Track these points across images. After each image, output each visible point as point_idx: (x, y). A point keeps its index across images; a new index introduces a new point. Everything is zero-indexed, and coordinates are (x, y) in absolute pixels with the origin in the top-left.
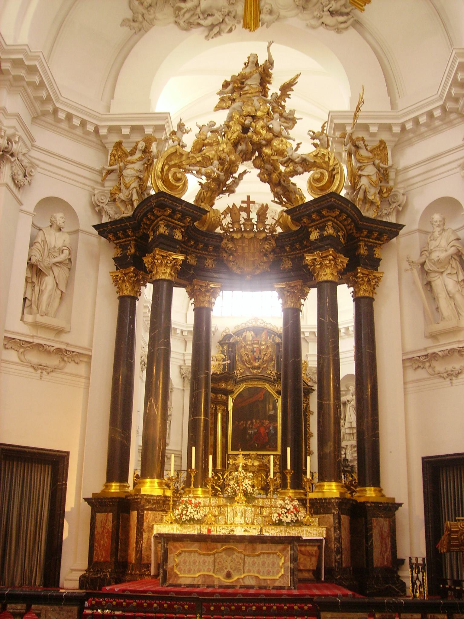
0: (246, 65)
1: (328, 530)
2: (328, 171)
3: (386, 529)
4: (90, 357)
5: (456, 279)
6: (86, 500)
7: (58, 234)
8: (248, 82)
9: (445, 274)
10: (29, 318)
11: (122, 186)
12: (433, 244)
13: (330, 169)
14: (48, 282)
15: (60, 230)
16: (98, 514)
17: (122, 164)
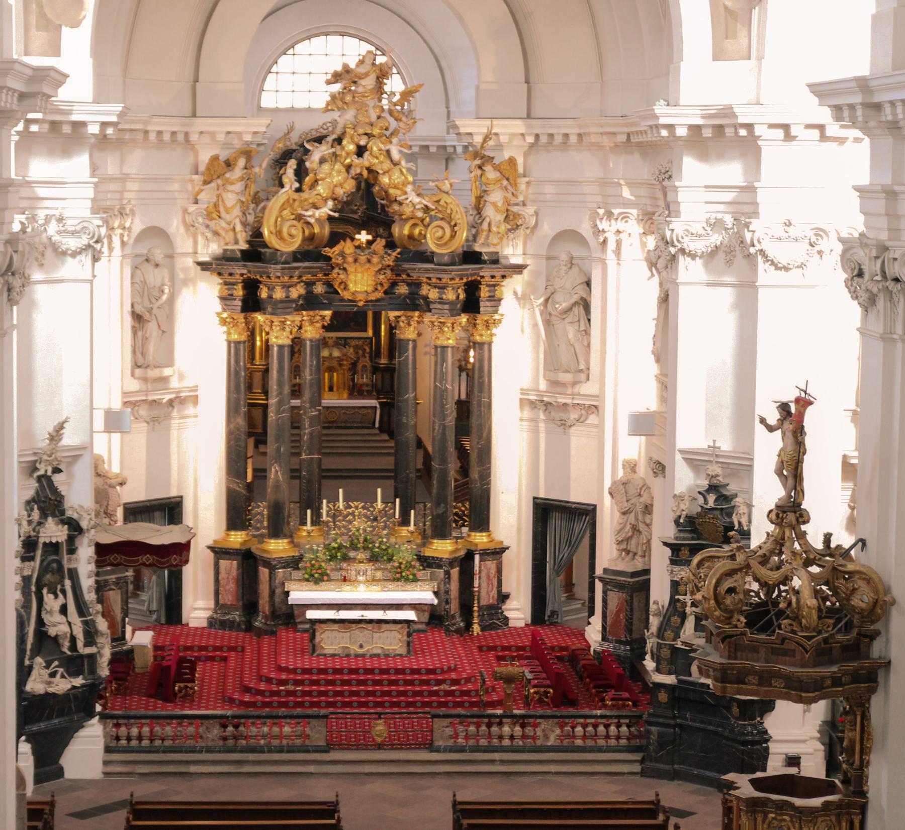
0: (361, 62)
1: (439, 585)
2: (449, 223)
3: (493, 570)
4: (197, 396)
5: (577, 328)
6: (209, 547)
7: (156, 270)
8: (363, 82)
9: (567, 320)
10: (138, 372)
11: (222, 209)
12: (558, 283)
13: (453, 223)
14: (152, 326)
15: (157, 265)
16: (221, 561)
17: (220, 182)
